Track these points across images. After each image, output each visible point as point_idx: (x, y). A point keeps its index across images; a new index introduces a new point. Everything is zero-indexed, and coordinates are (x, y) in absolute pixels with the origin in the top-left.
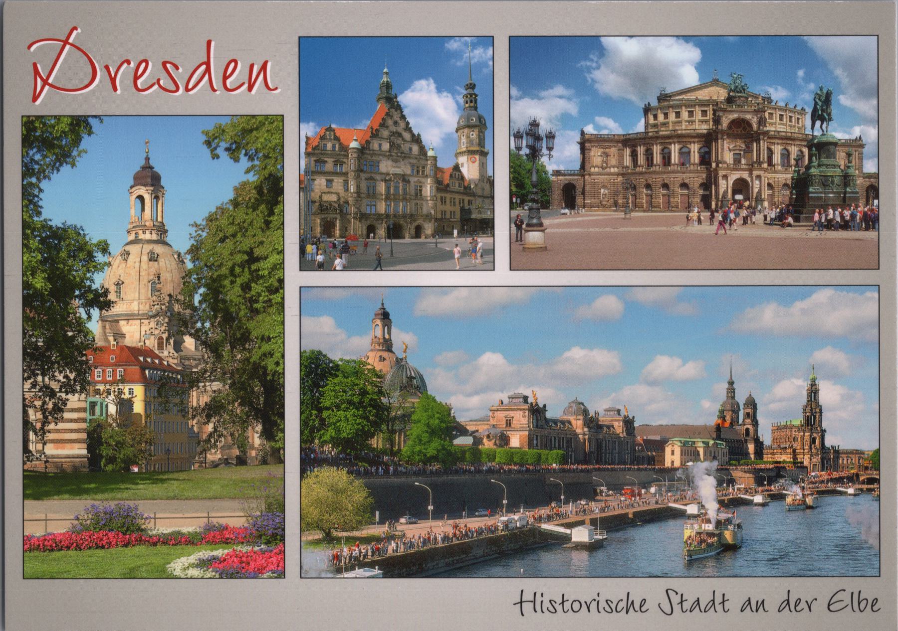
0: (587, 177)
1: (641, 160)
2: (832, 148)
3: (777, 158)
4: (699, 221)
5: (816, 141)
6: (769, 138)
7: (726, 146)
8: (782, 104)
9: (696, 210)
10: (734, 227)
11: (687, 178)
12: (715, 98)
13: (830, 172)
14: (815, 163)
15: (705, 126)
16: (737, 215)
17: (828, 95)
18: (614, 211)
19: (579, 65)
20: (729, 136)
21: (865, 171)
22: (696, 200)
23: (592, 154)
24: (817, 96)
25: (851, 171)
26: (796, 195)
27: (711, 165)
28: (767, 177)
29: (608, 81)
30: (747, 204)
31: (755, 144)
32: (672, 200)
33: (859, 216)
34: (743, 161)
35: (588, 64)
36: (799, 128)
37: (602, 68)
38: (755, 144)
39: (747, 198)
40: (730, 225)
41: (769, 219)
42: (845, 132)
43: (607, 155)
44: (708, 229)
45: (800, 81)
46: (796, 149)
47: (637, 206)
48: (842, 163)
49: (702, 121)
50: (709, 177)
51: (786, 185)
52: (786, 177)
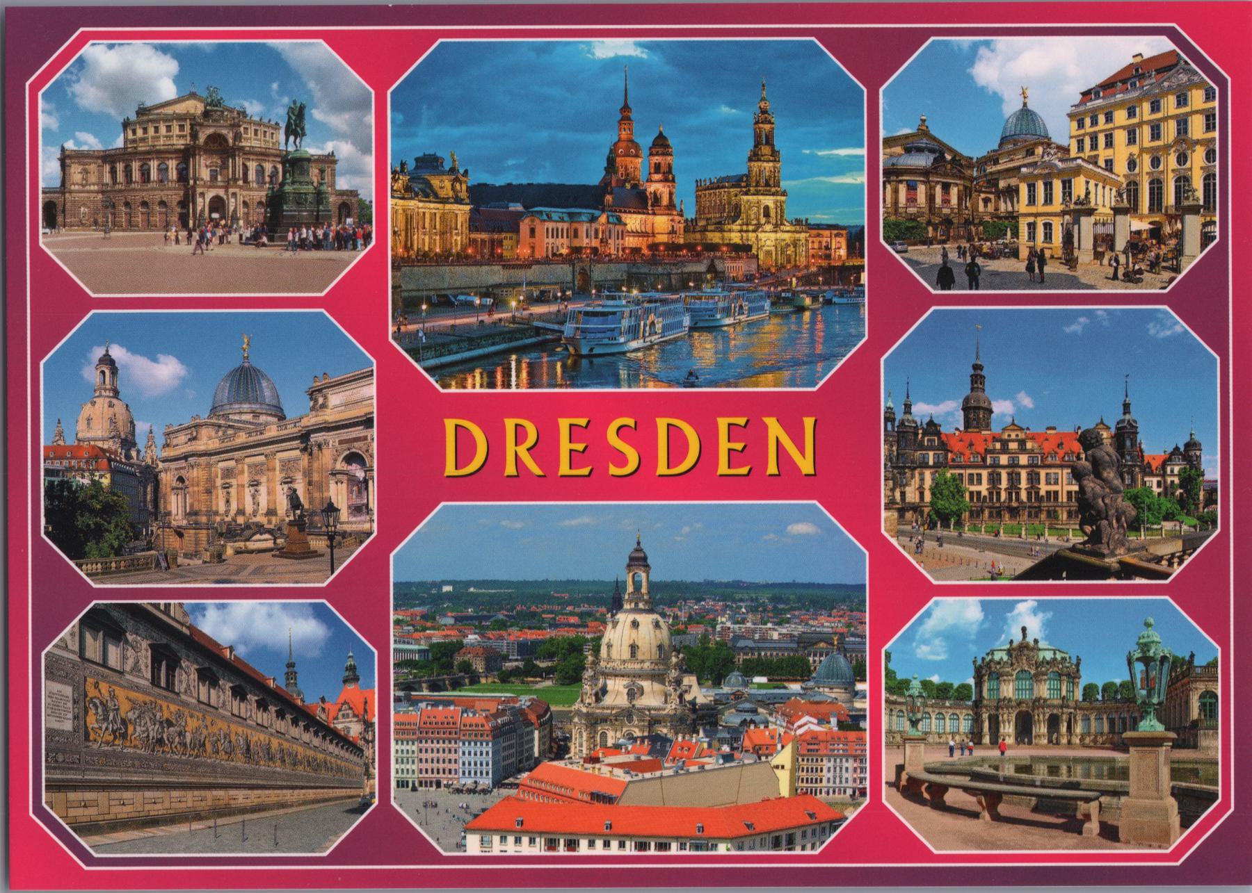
2: (306, 164)
3: (252, 175)
4: (177, 241)
7: (203, 162)
8: (256, 118)
9: (174, 229)
10: (211, 247)
16: (214, 234)
17: (302, 108)
24: (291, 110)
28: (243, 195)
30: (223, 222)
34: (219, 178)
39: (223, 217)
42: (318, 147)
44: (186, 249)
50: (186, 195)
51: (260, 203)
52: (261, 195)
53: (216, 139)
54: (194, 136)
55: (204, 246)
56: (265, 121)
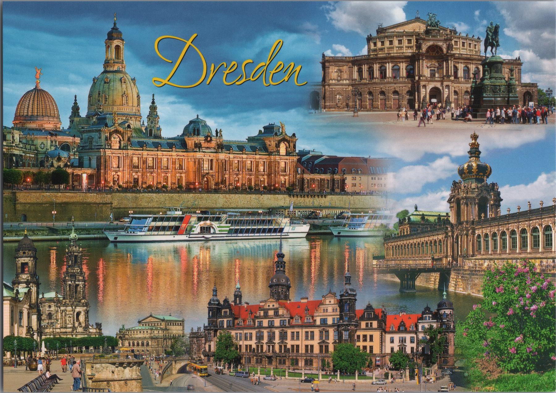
0: (327, 87)
1: (365, 75)
2: (499, 65)
3: (461, 73)
4: (407, 118)
5: (488, 61)
7: (425, 64)
8: (464, 35)
9: (404, 110)
10: (431, 121)
11: (397, 87)
12: (417, 30)
14: (488, 77)
15: (410, 51)
16: (433, 113)
17: (497, 28)
18: (346, 111)
19: (321, 8)
20: (427, 58)
21: (523, 81)
23: (330, 70)
24: (489, 29)
25: (513, 82)
26: (474, 98)
27: (415, 79)
28: (454, 86)
30: (440, 105)
31: (445, 63)
32: (387, 103)
33: (518, 113)
34: (437, 75)
35: (327, 7)
36: (476, 51)
37: (338, 9)
38: (445, 63)
40: (428, 120)
41: (455, 116)
42: (508, 55)
45: (476, 19)
46: (474, 66)
47: (363, 107)
48: (506, 76)
50: (413, 87)
51: (467, 92)
52: (468, 86)
55: (426, 121)
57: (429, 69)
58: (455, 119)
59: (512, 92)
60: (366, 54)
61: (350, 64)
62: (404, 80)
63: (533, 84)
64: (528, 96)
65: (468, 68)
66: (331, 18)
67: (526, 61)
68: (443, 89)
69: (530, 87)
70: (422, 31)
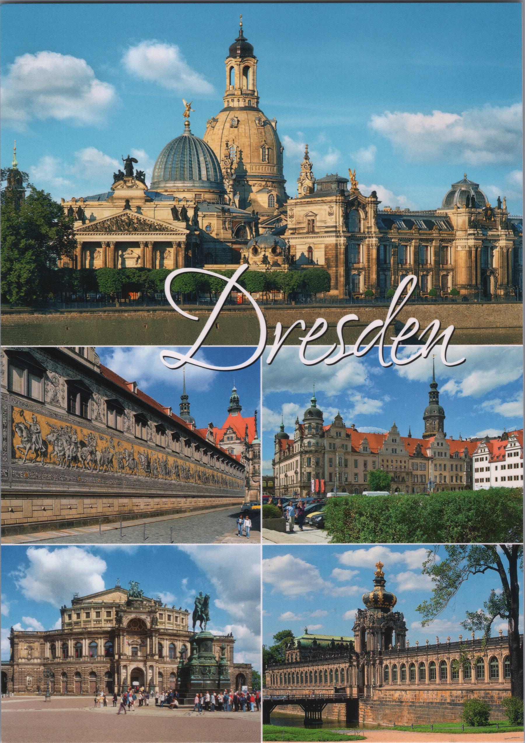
2: (209, 643)
3: (166, 652)
4: (105, 703)
6: (160, 635)
7: (126, 641)
8: (170, 607)
9: (102, 694)
10: (132, 708)
11: (93, 667)
12: (117, 601)
13: (207, 662)
16: (134, 698)
22: (102, 686)
24: (198, 600)
25: (224, 662)
26: (181, 681)
27: (114, 658)
28: (158, 667)
29: (33, 587)
30: (142, 689)
31: (148, 640)
32: (83, 686)
33: (230, 699)
34: (139, 654)
36: (183, 626)
37: (28, 576)
38: (148, 640)
40: (129, 706)
41: (159, 701)
42: (219, 630)
43: (31, 648)
49: (107, 621)
50: (112, 667)
51: (173, 673)
52: (174, 667)
53: (137, 623)
54: (119, 620)
55: (127, 708)
56: (177, 608)
57: (131, 647)
58: (159, 705)
59: (222, 674)
60: (60, 628)
61: (42, 640)
62: (102, 660)
63: (246, 665)
64: (241, 679)
65: (174, 645)
66: (20, 586)
67: (238, 637)
68: (146, 670)
69: (243, 668)
70: (123, 602)
